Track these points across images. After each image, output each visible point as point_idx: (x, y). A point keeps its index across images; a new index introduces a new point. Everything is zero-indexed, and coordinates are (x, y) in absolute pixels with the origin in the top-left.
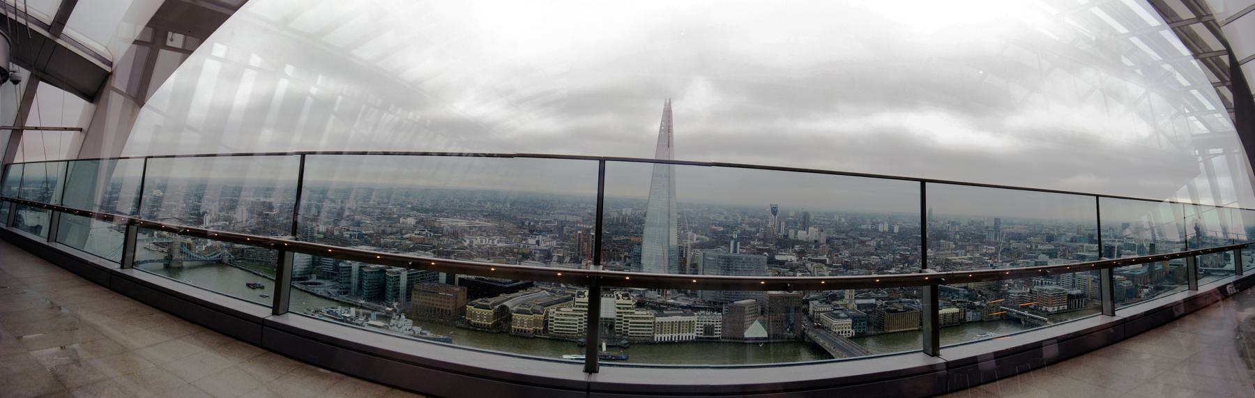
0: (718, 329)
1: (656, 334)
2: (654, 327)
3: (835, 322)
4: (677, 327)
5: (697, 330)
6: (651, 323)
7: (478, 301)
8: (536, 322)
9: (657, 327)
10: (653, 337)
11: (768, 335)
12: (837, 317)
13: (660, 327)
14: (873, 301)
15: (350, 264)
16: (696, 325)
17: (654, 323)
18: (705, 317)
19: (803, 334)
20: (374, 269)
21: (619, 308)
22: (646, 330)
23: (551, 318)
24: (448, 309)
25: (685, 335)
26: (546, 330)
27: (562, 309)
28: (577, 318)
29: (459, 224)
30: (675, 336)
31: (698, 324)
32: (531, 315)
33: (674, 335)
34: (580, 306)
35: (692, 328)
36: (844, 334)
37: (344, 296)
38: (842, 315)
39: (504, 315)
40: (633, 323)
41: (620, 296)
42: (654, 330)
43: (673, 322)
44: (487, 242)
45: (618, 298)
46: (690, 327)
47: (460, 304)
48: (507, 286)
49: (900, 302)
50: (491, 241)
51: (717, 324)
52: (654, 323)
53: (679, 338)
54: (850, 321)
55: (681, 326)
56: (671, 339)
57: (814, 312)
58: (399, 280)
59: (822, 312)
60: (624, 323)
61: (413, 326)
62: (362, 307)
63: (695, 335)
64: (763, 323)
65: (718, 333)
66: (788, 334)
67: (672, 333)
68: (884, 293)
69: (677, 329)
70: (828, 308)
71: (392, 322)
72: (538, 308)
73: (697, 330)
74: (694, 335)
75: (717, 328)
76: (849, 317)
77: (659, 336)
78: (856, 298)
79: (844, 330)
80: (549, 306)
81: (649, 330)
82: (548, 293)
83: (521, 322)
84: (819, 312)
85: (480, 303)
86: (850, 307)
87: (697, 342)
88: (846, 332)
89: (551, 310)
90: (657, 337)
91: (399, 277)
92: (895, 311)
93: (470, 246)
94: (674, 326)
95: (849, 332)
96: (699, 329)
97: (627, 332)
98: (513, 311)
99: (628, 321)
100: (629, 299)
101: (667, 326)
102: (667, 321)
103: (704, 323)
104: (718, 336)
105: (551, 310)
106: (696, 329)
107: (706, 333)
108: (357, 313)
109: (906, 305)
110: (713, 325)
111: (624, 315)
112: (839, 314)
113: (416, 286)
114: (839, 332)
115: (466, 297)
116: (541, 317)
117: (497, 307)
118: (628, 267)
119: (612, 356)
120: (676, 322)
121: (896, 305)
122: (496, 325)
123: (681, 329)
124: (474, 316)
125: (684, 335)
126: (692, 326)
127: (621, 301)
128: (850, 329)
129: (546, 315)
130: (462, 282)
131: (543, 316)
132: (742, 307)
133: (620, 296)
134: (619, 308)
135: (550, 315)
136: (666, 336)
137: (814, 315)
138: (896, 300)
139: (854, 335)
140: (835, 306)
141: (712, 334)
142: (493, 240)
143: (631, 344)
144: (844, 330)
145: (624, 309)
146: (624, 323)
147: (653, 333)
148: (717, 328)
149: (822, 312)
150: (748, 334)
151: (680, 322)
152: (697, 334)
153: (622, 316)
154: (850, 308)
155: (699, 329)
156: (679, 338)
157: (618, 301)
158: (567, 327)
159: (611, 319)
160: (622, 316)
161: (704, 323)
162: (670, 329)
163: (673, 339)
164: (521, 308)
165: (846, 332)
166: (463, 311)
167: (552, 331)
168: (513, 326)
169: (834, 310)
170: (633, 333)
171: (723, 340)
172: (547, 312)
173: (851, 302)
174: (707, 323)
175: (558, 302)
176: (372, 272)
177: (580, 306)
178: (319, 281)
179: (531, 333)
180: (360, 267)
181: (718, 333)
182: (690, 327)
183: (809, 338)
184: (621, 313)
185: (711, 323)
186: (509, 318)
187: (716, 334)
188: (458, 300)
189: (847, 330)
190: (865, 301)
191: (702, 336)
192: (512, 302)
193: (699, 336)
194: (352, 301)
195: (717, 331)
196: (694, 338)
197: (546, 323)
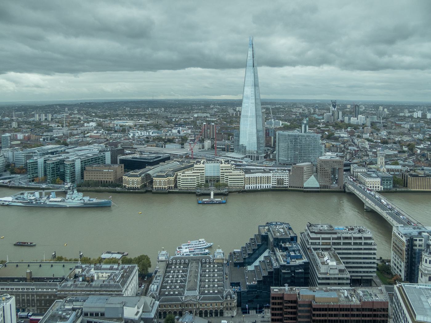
0: (287, 181)
1: (246, 185)
2: (245, 180)
3: (368, 180)
4: (260, 180)
5: (273, 182)
6: (242, 178)
7: (131, 173)
8: (169, 182)
9: (246, 180)
10: (244, 187)
11: (320, 186)
12: (370, 176)
13: (248, 180)
14: (399, 167)
15: (36, 160)
16: (272, 179)
17: (244, 178)
18: (278, 174)
19: (344, 187)
20: (54, 160)
21: (222, 170)
22: (239, 183)
23: (179, 178)
24: (110, 180)
25: (265, 186)
26: (176, 186)
27: (186, 173)
28: (195, 177)
29: (127, 124)
30: (258, 186)
31: (273, 178)
32: (166, 178)
33: (258, 185)
34: (197, 170)
35: (269, 181)
36: (377, 188)
37: (33, 183)
38: (374, 175)
39: (149, 179)
40: (231, 178)
41: (223, 162)
42: (245, 182)
43: (256, 177)
44: (145, 134)
45: (221, 163)
46: (268, 180)
47: (118, 177)
48: (152, 161)
49: (423, 170)
50: (147, 133)
51: (285, 178)
52: (244, 178)
53: (261, 187)
54: (379, 180)
55: (262, 180)
56: (256, 187)
57: (354, 172)
58: (74, 166)
59: (359, 172)
60: (225, 179)
61: (83, 196)
62: (43, 189)
63: (271, 185)
64: (316, 177)
65: (286, 183)
66: (335, 186)
67: (256, 184)
68: (410, 162)
69: (260, 181)
70: (364, 170)
71: (68, 196)
72: (171, 173)
73: (273, 182)
74: (270, 185)
75: (286, 180)
76: (378, 177)
77: (248, 186)
78: (386, 164)
79: (375, 186)
80: (178, 171)
81: (241, 183)
82: (178, 163)
83: (160, 183)
84: (357, 172)
85: (132, 174)
86: (382, 170)
87: (273, 190)
88: (376, 187)
89: (179, 174)
90: (247, 187)
91: (74, 163)
92: (417, 176)
93: (133, 137)
94: (258, 180)
95: (378, 187)
96: (274, 181)
97: (228, 184)
98: (153, 177)
99: (228, 177)
100: (229, 164)
101: (253, 180)
102: (253, 177)
103: (277, 177)
104: (287, 186)
105: (179, 174)
106: (272, 181)
107: (278, 184)
108: (41, 194)
109: (427, 172)
110: (283, 178)
111: (225, 174)
112: (371, 174)
113: (87, 168)
114: (371, 187)
115: (123, 171)
116: (172, 178)
117: (143, 175)
118: (233, 144)
119: (217, 201)
120: (259, 177)
121: (419, 171)
122: (142, 187)
123: (262, 181)
124: (128, 182)
125: (264, 185)
126: (269, 179)
127: (223, 165)
128: (379, 185)
129: (176, 178)
130: (122, 161)
131: (173, 177)
132: (302, 168)
133: (223, 162)
134: (222, 170)
135: (178, 177)
136: (252, 186)
137: (353, 174)
138: (420, 168)
139: (382, 189)
140: (368, 169)
141: (283, 184)
142: (149, 132)
143: (230, 192)
144: (375, 186)
145: (225, 169)
146: (225, 179)
147: (244, 184)
148: (286, 180)
149: (359, 172)
150: (305, 185)
151: (261, 177)
152: (273, 184)
153: (224, 174)
154: (381, 171)
155: (274, 181)
156: (261, 187)
157: (221, 165)
158: (189, 183)
159: (218, 177)
160: (224, 174)
161: (277, 177)
162: (255, 182)
163: (257, 188)
164: (159, 174)
165: (376, 187)
166: (121, 180)
167: (180, 187)
168: (154, 186)
169: (368, 171)
170: (231, 185)
171: (290, 188)
172: (177, 175)
173: (382, 166)
174: (279, 177)
175: (184, 168)
176: (53, 163)
177: (197, 170)
178: (12, 176)
179: (166, 189)
180: (45, 161)
181: (286, 184)
182: (268, 180)
183: (348, 189)
184: (224, 172)
185: (282, 178)
186: (152, 182)
187: (285, 185)
188: (118, 173)
189: (377, 186)
190: (393, 167)
191: (276, 186)
192: (152, 171)
193: (274, 186)
194: (38, 186)
195: (285, 182)
196: (271, 187)
197: (176, 181)
